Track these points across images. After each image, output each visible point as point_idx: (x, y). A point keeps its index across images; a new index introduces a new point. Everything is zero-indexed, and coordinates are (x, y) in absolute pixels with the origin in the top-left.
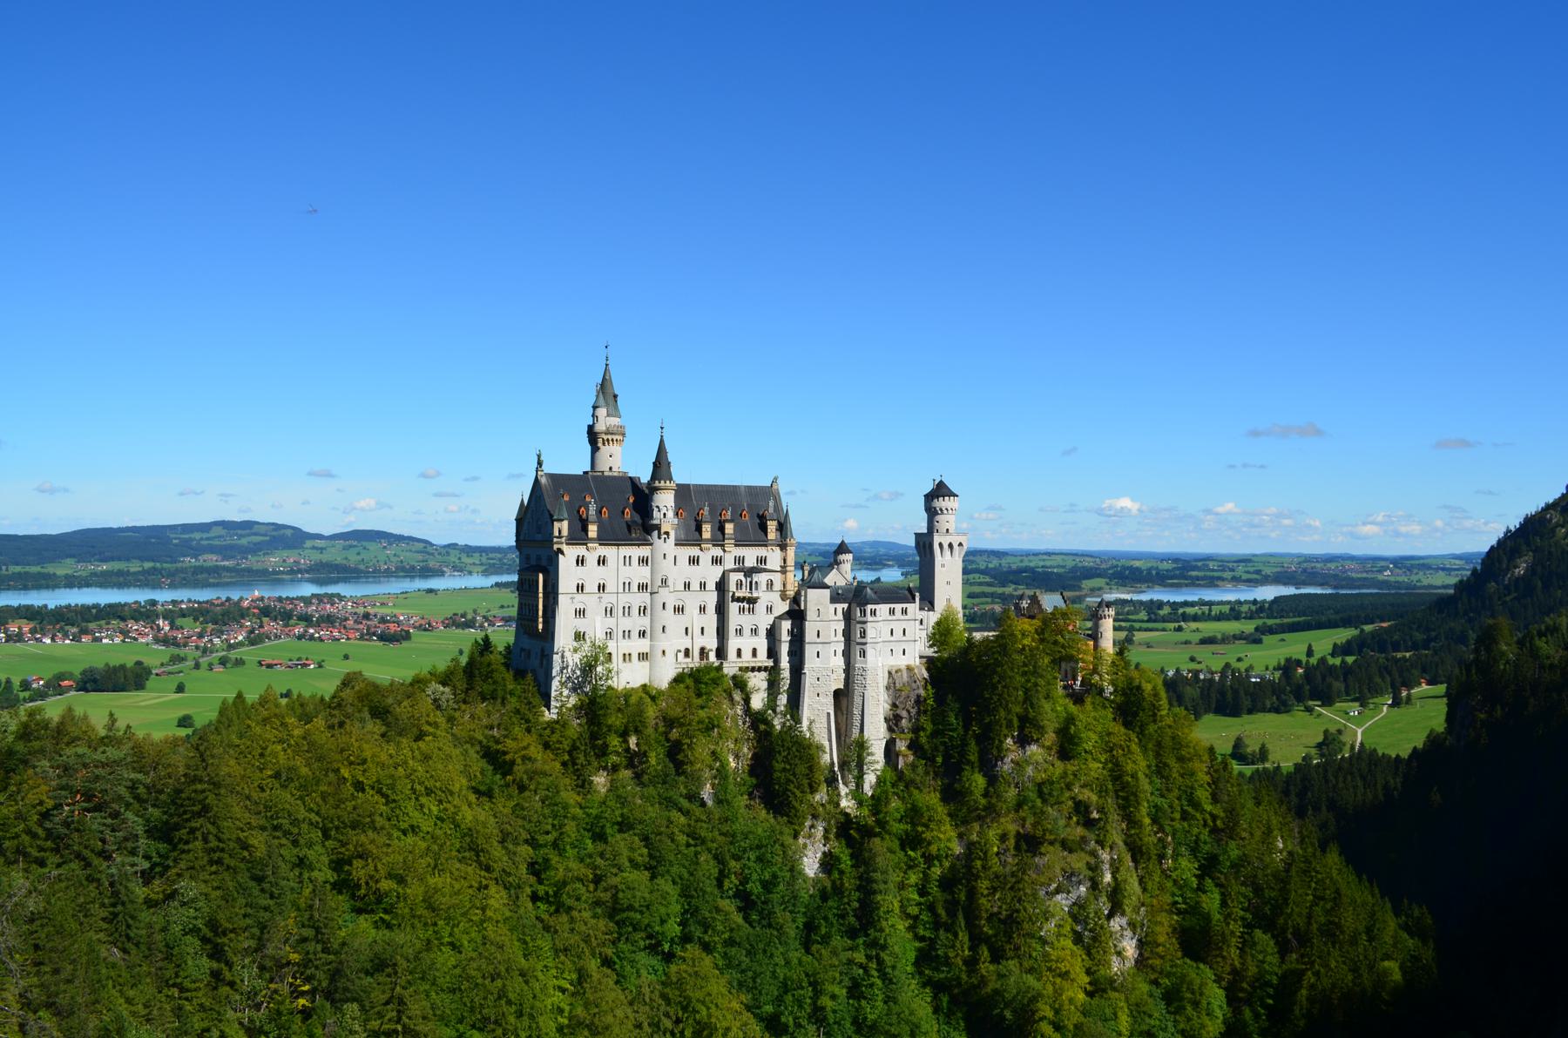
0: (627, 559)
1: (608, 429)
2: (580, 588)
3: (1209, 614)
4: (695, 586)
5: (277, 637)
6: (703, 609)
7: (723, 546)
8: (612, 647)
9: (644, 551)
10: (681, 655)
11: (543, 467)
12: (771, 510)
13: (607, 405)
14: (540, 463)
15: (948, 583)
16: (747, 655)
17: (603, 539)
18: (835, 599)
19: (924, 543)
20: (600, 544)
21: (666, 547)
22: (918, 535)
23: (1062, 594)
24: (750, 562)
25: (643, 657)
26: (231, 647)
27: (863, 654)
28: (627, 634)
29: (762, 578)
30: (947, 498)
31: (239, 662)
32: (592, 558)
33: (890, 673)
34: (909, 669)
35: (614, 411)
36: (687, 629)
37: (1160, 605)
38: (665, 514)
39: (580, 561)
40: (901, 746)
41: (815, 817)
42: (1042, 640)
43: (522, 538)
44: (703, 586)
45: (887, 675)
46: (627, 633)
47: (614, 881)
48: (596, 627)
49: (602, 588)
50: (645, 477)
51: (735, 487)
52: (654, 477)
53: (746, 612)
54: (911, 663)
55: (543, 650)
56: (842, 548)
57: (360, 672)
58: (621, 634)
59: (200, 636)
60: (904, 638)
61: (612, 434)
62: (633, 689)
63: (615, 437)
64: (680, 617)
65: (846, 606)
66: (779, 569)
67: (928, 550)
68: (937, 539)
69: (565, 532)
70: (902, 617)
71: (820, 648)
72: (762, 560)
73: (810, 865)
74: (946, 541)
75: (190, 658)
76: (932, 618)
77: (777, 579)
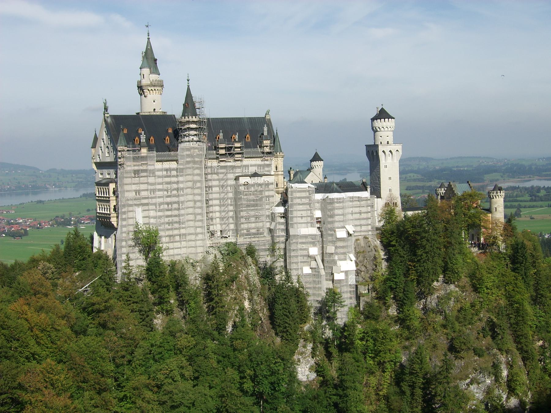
1: (151, 83)
12: (266, 133)
14: (106, 109)
15: (390, 178)
19: (372, 151)
22: (368, 146)
30: (386, 120)
34: (365, 238)
35: (154, 69)
37: (539, 189)
40: (363, 290)
41: (306, 340)
51: (240, 119)
52: (184, 115)
63: (156, 88)
68: (381, 149)
74: (387, 149)
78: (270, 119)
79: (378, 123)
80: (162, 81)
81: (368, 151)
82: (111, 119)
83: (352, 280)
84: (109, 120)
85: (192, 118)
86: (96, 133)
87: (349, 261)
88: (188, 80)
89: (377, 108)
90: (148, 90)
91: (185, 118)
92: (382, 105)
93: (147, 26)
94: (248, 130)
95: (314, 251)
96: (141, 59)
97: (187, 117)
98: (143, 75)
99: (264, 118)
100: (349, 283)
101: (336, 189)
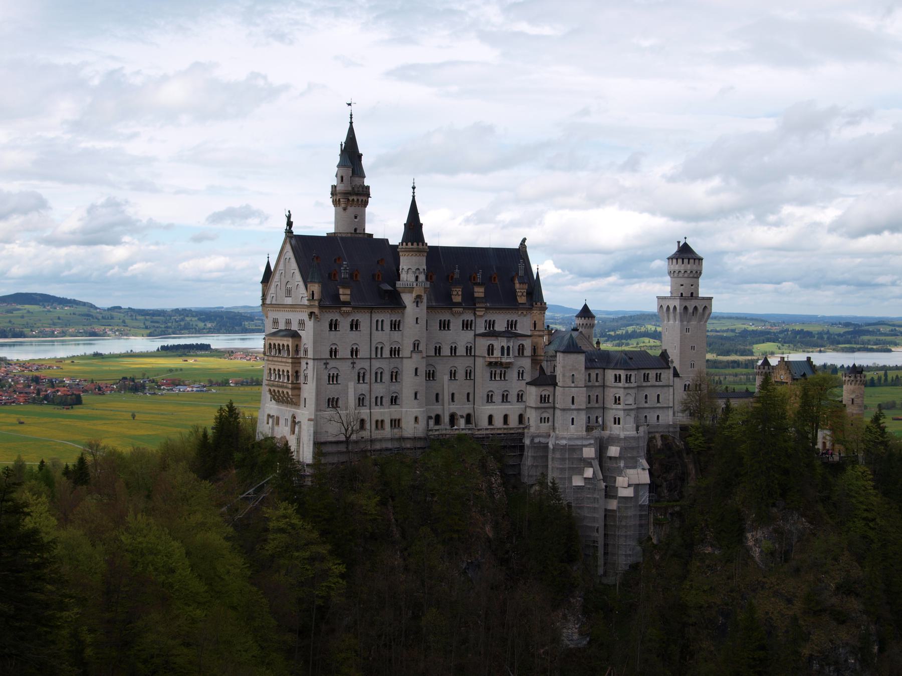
0: (380, 323)
1: (353, 188)
2: (333, 353)
3: (886, 379)
6: (453, 375)
7: (475, 311)
8: (364, 412)
9: (395, 318)
10: (432, 422)
11: (292, 229)
12: (521, 273)
14: (290, 224)
15: (693, 348)
16: (498, 422)
19: (668, 306)
20: (354, 308)
24: (500, 326)
28: (379, 401)
29: (513, 344)
36: (437, 395)
38: (417, 278)
39: (334, 326)
43: (268, 301)
44: (454, 350)
46: (379, 399)
49: (354, 352)
52: (407, 238)
55: (294, 417)
56: (585, 312)
58: (373, 400)
60: (658, 405)
61: (357, 194)
63: (360, 198)
64: (432, 383)
65: (599, 371)
66: (529, 334)
70: (657, 384)
71: (574, 415)
72: (512, 324)
77: (527, 343)
78: (526, 251)
79: (678, 266)
80: (368, 188)
81: (661, 306)
82: (297, 241)
83: (644, 499)
84: (293, 242)
85: (418, 245)
87: (640, 470)
88: (414, 188)
89: (679, 242)
90: (349, 200)
91: (407, 245)
92: (685, 238)
93: (349, 104)
94: (494, 267)
95: (589, 452)
96: (339, 152)
97: (409, 244)
98: (342, 177)
99: (519, 249)
100: (640, 503)
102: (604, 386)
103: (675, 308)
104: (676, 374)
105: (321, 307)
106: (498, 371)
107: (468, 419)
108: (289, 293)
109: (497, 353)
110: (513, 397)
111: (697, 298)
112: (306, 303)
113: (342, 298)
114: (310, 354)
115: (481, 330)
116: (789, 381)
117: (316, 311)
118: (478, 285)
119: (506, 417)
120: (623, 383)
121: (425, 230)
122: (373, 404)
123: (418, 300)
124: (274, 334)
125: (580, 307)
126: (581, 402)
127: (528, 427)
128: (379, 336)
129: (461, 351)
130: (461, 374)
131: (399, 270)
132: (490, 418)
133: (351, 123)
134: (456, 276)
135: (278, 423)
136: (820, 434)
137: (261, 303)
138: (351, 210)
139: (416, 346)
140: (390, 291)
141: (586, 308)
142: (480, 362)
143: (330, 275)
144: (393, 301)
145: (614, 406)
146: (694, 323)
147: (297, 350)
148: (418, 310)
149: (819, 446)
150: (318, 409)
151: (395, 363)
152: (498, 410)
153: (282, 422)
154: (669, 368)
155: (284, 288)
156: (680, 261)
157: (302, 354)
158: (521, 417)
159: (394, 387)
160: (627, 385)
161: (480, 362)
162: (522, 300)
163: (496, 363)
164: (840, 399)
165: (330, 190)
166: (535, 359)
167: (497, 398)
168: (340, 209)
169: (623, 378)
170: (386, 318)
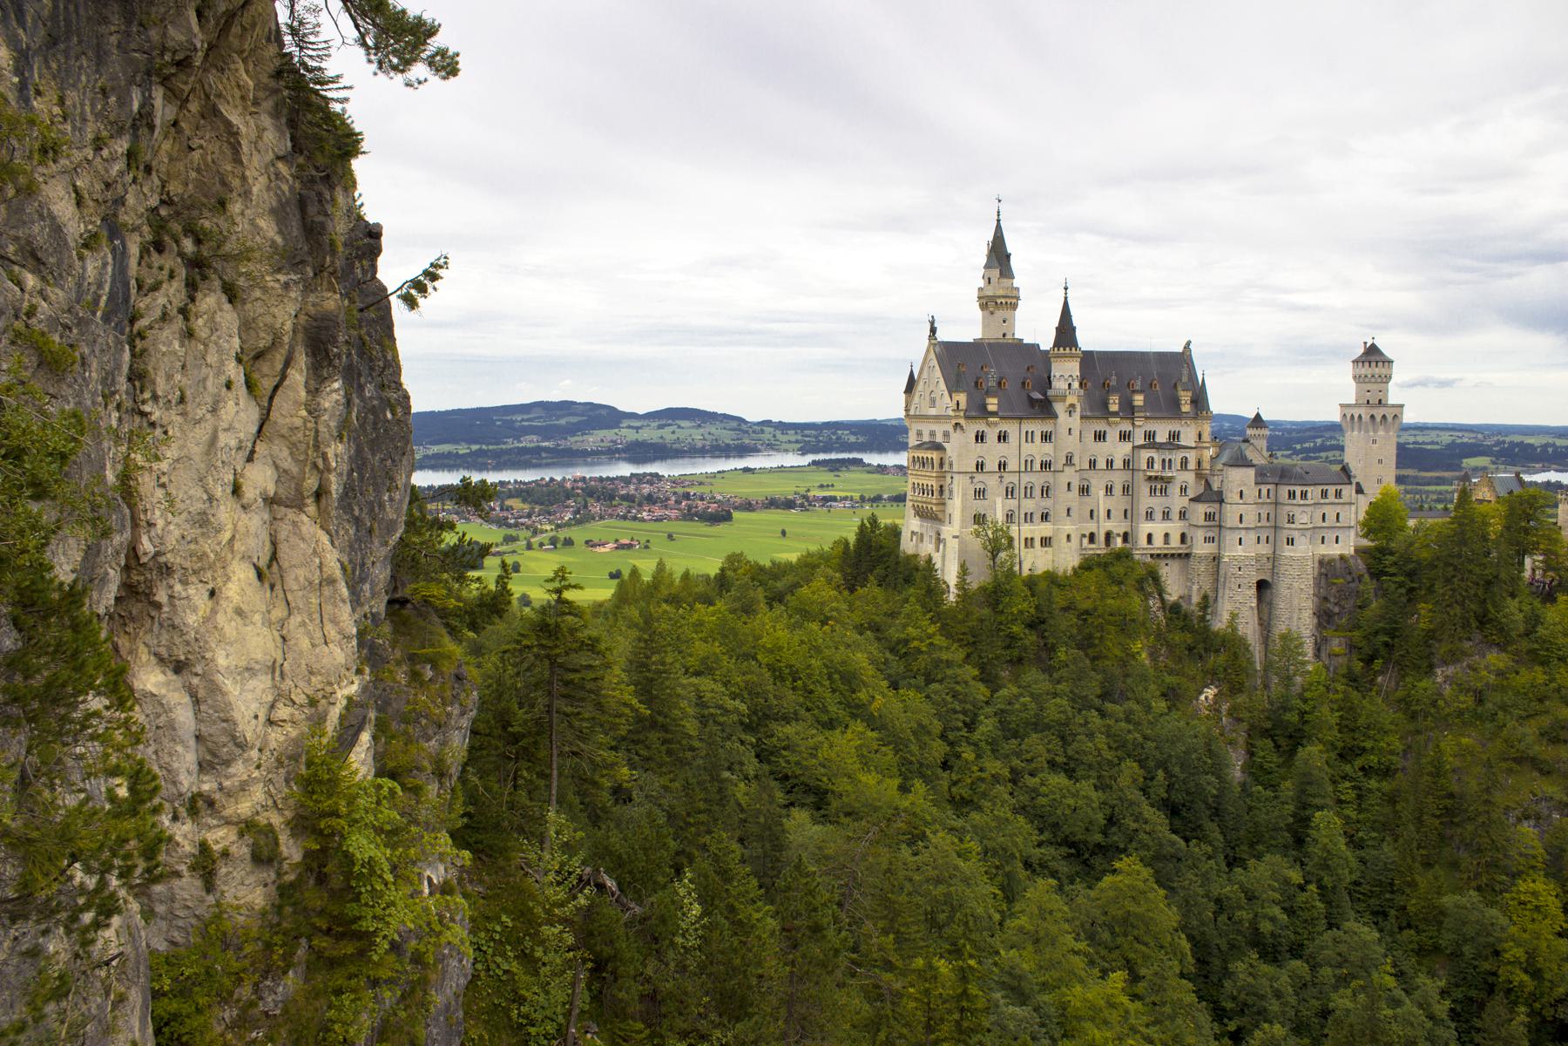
2: (980, 466)
4: (1101, 464)
5: (602, 518)
6: (1109, 490)
9: (1047, 426)
10: (1086, 541)
12: (1185, 379)
13: (1001, 265)
14: (933, 330)
15: (1380, 461)
16: (1158, 541)
17: (1006, 414)
18: (1262, 476)
20: (1001, 418)
21: (1068, 422)
22: (1342, 406)
23: (1517, 475)
24: (1161, 438)
25: (1046, 542)
26: (558, 526)
27: (1290, 542)
28: (1029, 518)
29: (1177, 457)
31: (569, 542)
32: (992, 435)
33: (1321, 563)
34: (1342, 557)
36: (1092, 511)
39: (980, 437)
42: (1508, 528)
43: (912, 413)
44: (1110, 463)
45: (1317, 565)
47: (1032, 782)
48: (998, 508)
49: (1002, 466)
50: (1046, 341)
51: (1143, 354)
52: (1058, 343)
53: (1158, 494)
54: (1346, 552)
57: (742, 554)
58: (1023, 516)
59: (529, 516)
62: (1038, 576)
64: (1086, 499)
65: (1271, 487)
66: (1194, 445)
67: (1356, 425)
69: (963, 406)
71: (1243, 534)
72: (1174, 436)
73: (1236, 773)
75: (521, 537)
76: (1363, 504)
79: (1365, 370)
80: (1018, 289)
84: (937, 349)
86: (912, 372)
88: (1066, 289)
96: (985, 251)
101: (1301, 477)
102: (1276, 504)
103: (1360, 416)
104: (1359, 490)
105: (967, 418)
106: (1159, 487)
107: (1125, 537)
108: (933, 402)
109: (1157, 466)
110: (1175, 515)
111: (1386, 405)
112: (951, 413)
113: (991, 408)
114: (955, 469)
115: (1140, 441)
116: (1493, 499)
117: (962, 422)
118: (1134, 392)
119: (1167, 535)
120: (1298, 500)
121: (1079, 335)
122: (1022, 521)
123: (1071, 410)
124: (918, 447)
125: (1252, 416)
126: (1251, 520)
127: (1190, 547)
128: (1028, 449)
129: (1118, 464)
130: (1118, 490)
131: (1049, 377)
132: (1150, 537)
133: (998, 221)
134: (1113, 383)
135: (922, 541)
136: (1528, 561)
137: (904, 413)
138: (1000, 314)
139: (1069, 460)
140: (1041, 401)
141: (1258, 415)
142: (1140, 477)
143: (976, 383)
144: (1043, 408)
145: (1287, 526)
146: (1381, 433)
147: (941, 465)
148: (1070, 420)
149: (1527, 574)
150: (963, 525)
151: (1047, 477)
152: (1158, 528)
153: (926, 538)
154: (1351, 483)
155: (928, 398)
156: (1367, 364)
157: (946, 468)
158: (1183, 537)
159: (1047, 503)
160: (1302, 502)
161: (1140, 477)
162: (1186, 408)
163: (1156, 477)
164: (1554, 520)
165: (975, 295)
166: (1199, 474)
167: (1158, 515)
168: (987, 313)
169: (1298, 494)
170: (1037, 427)
